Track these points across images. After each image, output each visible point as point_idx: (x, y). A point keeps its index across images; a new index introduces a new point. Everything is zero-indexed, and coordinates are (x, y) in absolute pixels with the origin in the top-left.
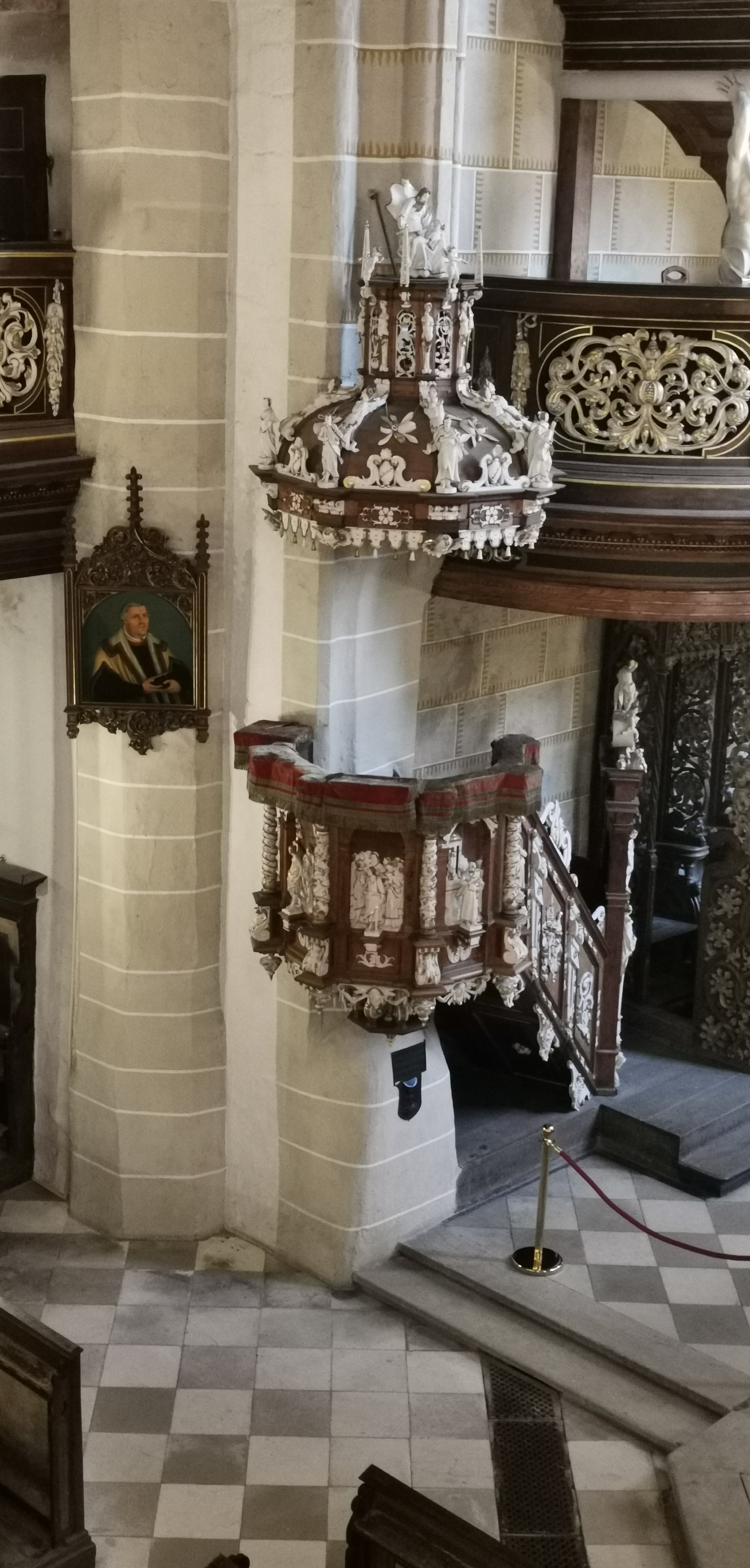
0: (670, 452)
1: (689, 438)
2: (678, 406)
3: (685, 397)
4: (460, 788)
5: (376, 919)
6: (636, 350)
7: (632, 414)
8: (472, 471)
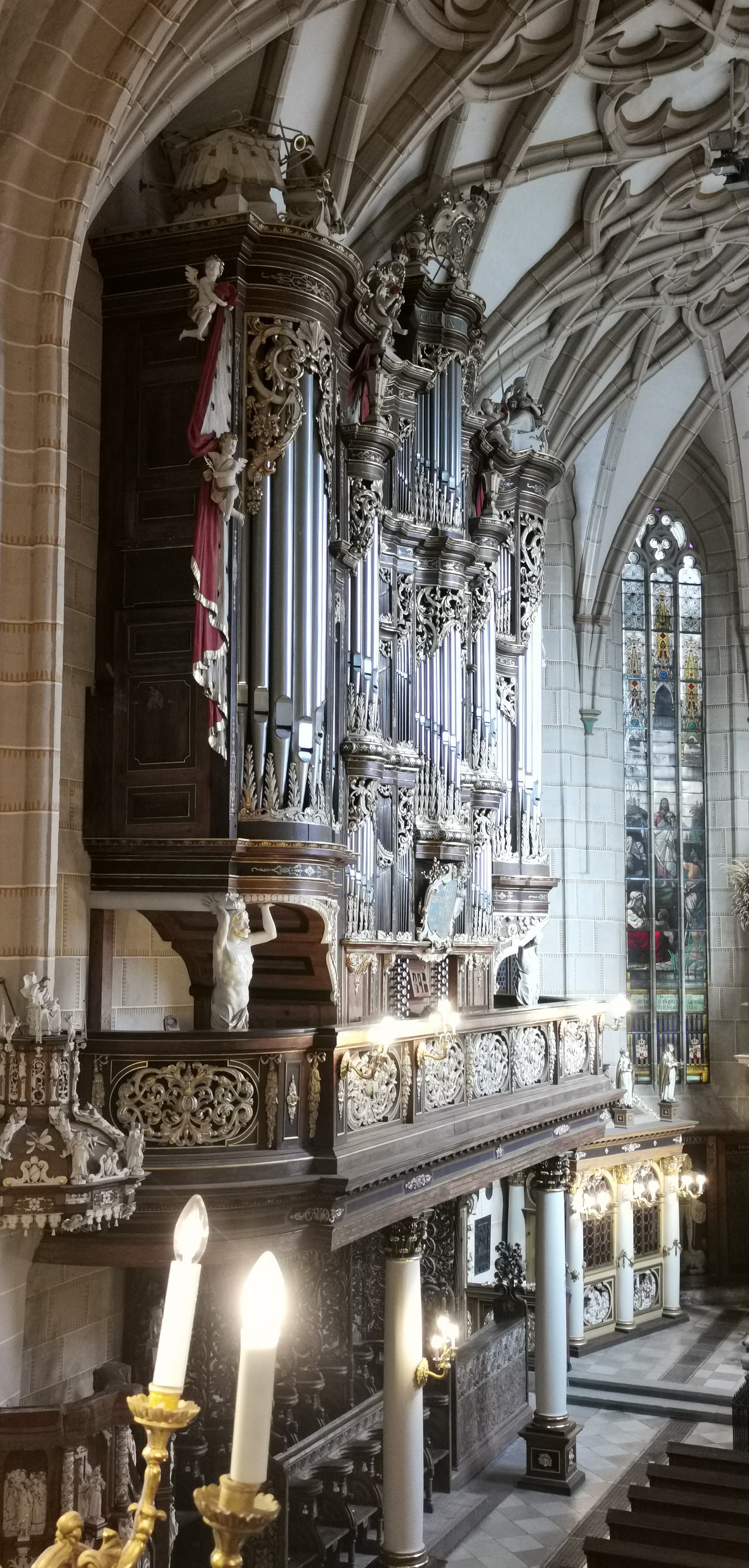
0: (203, 1144)
1: (216, 1133)
2: (207, 1112)
3: (211, 1105)
4: (90, 1407)
5: (26, 1527)
6: (178, 1076)
7: (177, 1119)
8: (94, 1167)
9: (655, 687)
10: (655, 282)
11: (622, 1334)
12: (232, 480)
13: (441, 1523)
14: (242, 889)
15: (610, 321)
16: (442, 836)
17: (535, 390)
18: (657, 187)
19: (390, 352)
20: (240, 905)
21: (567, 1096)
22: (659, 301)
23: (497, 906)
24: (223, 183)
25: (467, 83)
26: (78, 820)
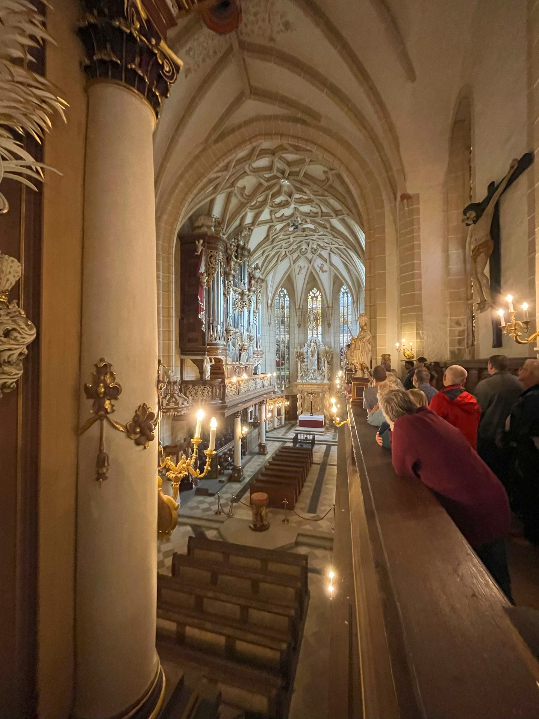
8: (183, 404)
9: (281, 319)
10: (282, 246)
11: (275, 429)
12: (205, 281)
13: (244, 461)
14: (208, 355)
15: (273, 253)
16: (244, 345)
17: (260, 265)
18: (282, 229)
19: (234, 258)
20: (208, 358)
21: (265, 390)
22: (282, 250)
23: (254, 357)
24: (203, 225)
25: (247, 209)
26: (178, 343)
